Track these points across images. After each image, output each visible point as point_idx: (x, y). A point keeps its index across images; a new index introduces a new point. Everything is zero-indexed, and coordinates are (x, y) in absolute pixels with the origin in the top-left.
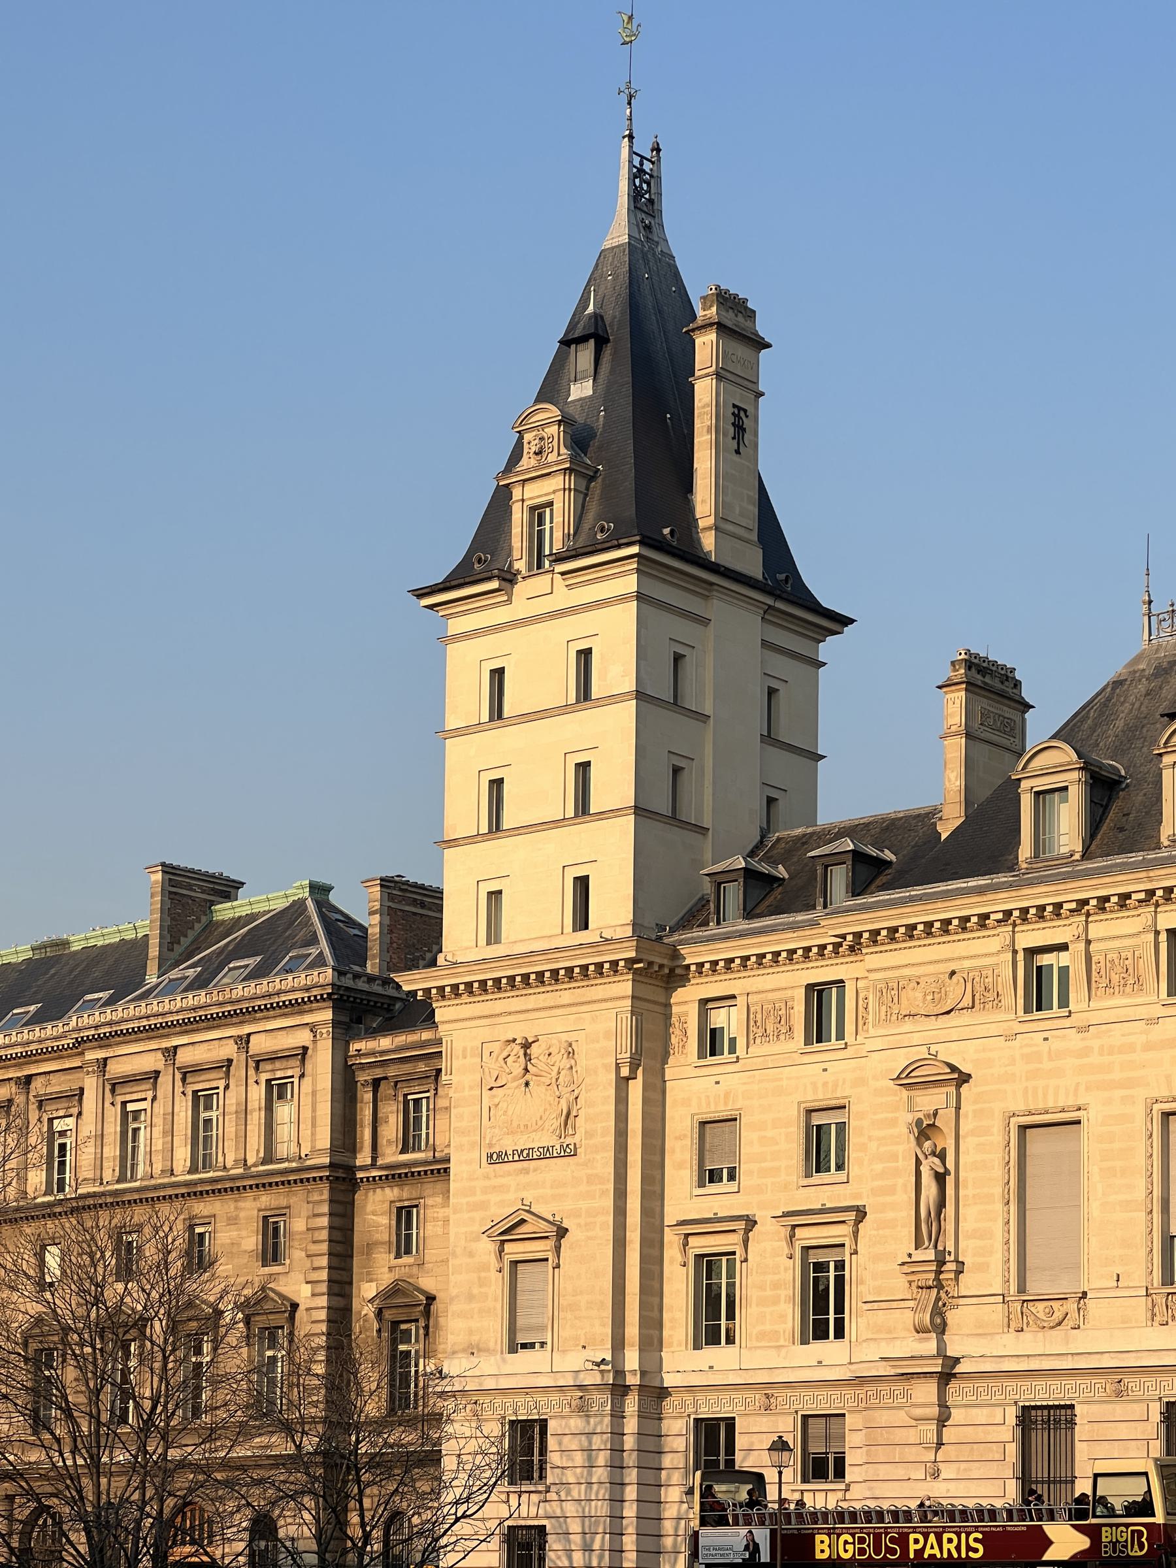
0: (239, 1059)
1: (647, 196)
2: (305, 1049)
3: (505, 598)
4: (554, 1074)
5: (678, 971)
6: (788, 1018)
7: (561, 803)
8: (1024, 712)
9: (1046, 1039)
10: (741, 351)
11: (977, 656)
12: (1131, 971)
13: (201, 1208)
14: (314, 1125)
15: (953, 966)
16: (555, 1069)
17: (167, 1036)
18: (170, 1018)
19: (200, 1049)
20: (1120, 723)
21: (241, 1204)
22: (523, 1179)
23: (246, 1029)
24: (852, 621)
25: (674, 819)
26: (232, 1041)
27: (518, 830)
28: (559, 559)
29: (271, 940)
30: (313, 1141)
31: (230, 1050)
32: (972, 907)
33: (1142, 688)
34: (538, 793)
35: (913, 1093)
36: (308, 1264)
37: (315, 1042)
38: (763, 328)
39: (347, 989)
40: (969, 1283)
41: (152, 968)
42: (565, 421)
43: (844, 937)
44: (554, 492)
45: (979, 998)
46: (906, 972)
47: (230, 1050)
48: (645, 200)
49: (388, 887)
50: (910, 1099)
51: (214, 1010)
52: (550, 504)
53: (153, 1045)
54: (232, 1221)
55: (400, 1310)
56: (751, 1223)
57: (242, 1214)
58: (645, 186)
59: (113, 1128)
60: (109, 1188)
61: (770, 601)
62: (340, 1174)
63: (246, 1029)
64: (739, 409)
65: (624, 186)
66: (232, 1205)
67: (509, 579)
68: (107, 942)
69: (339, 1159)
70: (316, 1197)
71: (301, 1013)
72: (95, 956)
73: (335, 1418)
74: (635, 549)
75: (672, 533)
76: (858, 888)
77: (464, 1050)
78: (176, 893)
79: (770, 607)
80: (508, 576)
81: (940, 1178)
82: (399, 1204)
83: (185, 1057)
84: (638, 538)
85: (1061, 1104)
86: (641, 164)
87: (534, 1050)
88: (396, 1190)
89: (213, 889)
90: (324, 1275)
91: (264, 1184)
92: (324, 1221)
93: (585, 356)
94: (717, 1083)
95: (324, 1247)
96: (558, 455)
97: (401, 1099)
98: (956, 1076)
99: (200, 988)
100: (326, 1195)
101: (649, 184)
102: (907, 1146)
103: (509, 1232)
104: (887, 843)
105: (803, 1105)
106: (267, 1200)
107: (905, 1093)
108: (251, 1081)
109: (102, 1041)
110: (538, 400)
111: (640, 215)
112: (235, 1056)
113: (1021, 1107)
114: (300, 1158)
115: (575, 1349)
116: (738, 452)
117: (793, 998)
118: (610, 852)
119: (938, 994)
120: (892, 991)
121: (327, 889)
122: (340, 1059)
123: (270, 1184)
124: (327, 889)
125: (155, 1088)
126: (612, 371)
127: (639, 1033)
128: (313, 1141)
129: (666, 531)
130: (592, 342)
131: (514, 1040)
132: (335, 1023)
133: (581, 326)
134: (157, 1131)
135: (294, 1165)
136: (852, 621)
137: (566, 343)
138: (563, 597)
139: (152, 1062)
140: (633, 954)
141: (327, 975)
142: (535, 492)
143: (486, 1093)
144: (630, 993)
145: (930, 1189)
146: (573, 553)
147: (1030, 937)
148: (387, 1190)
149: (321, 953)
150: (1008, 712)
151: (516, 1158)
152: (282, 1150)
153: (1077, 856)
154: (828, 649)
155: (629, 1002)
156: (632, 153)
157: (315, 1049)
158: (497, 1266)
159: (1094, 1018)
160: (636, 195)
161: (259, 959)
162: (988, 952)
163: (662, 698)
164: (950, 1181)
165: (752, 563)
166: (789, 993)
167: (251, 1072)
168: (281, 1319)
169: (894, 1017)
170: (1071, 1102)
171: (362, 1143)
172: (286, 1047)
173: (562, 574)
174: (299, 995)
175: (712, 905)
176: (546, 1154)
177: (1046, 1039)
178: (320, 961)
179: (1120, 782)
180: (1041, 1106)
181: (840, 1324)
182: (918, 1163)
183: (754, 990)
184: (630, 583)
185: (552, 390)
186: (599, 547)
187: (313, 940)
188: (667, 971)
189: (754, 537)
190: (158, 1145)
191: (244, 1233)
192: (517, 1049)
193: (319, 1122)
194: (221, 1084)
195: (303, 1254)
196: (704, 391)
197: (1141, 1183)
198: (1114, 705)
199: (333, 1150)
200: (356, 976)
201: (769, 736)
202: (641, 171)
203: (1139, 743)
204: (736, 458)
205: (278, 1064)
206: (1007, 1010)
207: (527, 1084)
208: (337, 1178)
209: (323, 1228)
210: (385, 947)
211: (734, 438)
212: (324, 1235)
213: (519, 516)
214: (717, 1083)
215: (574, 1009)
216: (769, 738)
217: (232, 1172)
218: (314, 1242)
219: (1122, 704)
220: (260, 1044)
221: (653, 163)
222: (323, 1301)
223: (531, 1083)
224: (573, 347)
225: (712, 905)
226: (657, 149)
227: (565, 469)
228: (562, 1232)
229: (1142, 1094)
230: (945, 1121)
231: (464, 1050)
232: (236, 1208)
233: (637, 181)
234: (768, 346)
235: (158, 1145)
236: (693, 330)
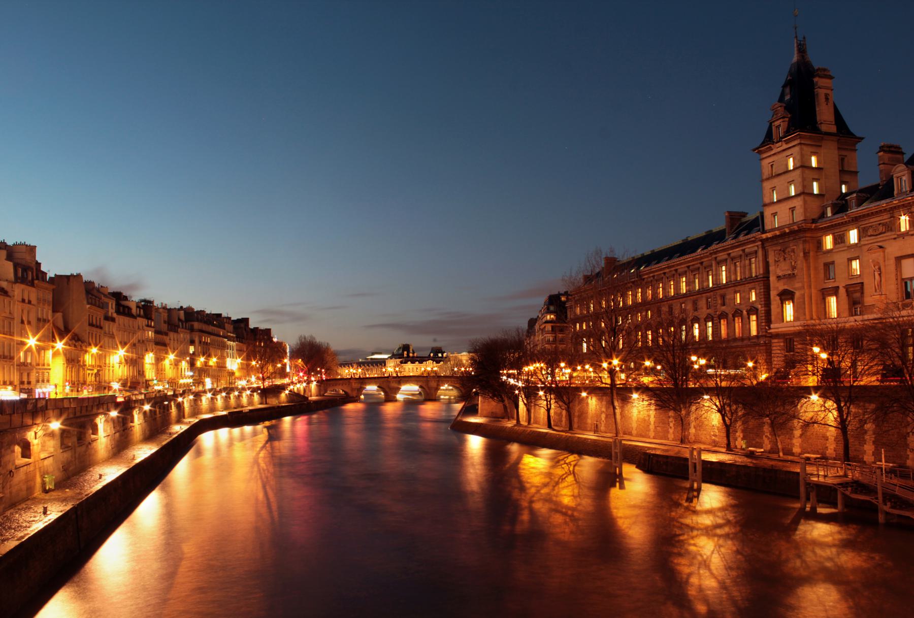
19: (736, 252)
24: (862, 138)
83: (732, 255)
106: (750, 286)
109: (715, 253)
165: (833, 129)
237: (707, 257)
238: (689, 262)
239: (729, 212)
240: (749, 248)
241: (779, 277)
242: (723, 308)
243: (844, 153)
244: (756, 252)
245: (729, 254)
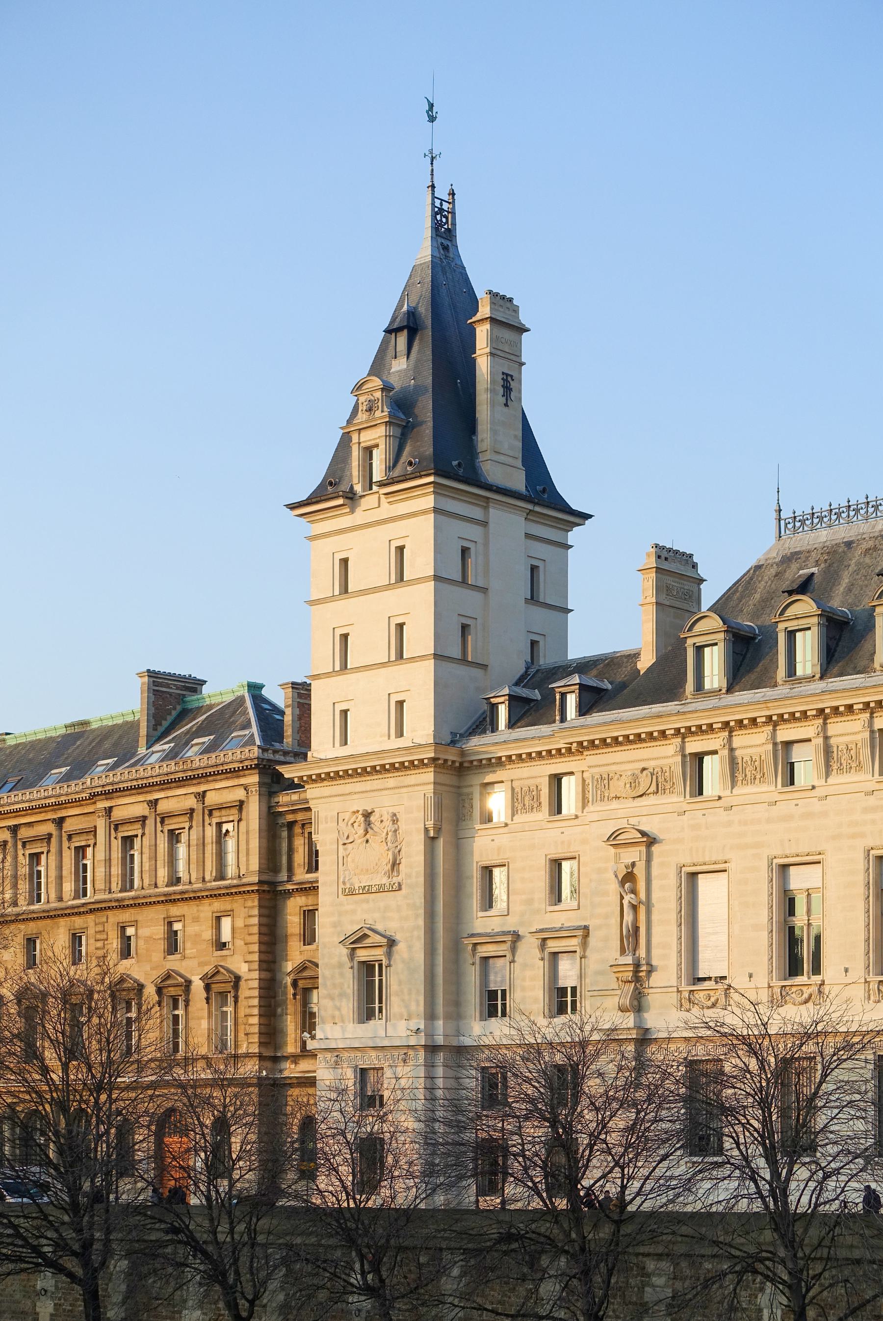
0: (198, 807)
1: (446, 227)
2: (242, 803)
3: (348, 510)
4: (384, 834)
5: (466, 765)
6: (539, 796)
7: (382, 652)
8: (699, 584)
9: (704, 815)
10: (507, 334)
11: (663, 548)
12: (758, 769)
13: (175, 910)
14: (248, 854)
16: (385, 831)
17: (150, 792)
18: (151, 780)
19: (175, 801)
20: (757, 596)
21: (201, 908)
22: (365, 906)
23: (202, 788)
24: (590, 516)
25: (463, 660)
26: (193, 796)
27: (357, 669)
28: (382, 484)
29: (222, 722)
30: (248, 865)
31: (191, 802)
32: (655, 727)
33: (773, 571)
34: (371, 645)
35: (619, 850)
36: (245, 947)
37: (247, 797)
38: (524, 318)
39: (269, 760)
40: (656, 980)
41: (143, 741)
42: (386, 388)
43: (571, 744)
44: (379, 437)
45: (659, 785)
46: (614, 768)
47: (191, 802)
48: (444, 232)
49: (297, 689)
50: (616, 854)
51: (180, 775)
52: (377, 446)
53: (141, 798)
54: (196, 920)
55: (308, 981)
56: (516, 937)
57: (202, 915)
58: (444, 220)
59: (117, 854)
60: (114, 895)
61: (530, 507)
62: (266, 888)
63: (202, 788)
64: (507, 375)
65: (428, 223)
66: (195, 909)
67: (351, 497)
68: (115, 723)
69: (265, 877)
70: (249, 903)
71: (238, 777)
72: (107, 733)
73: (267, 1053)
74: (431, 479)
75: (459, 465)
76: (584, 710)
77: (326, 818)
78: (157, 691)
79: (530, 510)
80: (350, 495)
81: (634, 908)
82: (305, 908)
83: (162, 807)
84: (432, 471)
85: (714, 859)
86: (441, 204)
87: (372, 818)
88: (304, 898)
89: (184, 686)
90: (256, 957)
91: (214, 896)
92: (255, 920)
93: (402, 339)
94: (493, 840)
95: (256, 938)
96: (382, 414)
97: (306, 835)
98: (645, 839)
99: (171, 759)
100: (256, 903)
101: (447, 218)
102: (614, 887)
103: (358, 940)
104: (607, 675)
105: (549, 857)
106: (218, 905)
107: (612, 850)
108: (206, 823)
109: (108, 795)
110: (369, 375)
111: (440, 240)
112: (195, 807)
113: (688, 861)
114: (239, 877)
115: (403, 1019)
116: (506, 405)
117: (541, 784)
118: (418, 685)
119: (634, 782)
120: (605, 780)
121: (260, 687)
122: (265, 809)
123: (220, 895)
124: (260, 687)
126: (419, 352)
127: (439, 806)
128: (248, 865)
129: (455, 463)
130: (405, 332)
131: (358, 811)
132: (261, 784)
133: (398, 320)
134: (146, 857)
135: (235, 882)
136: (590, 516)
137: (388, 331)
138: (387, 510)
139: (141, 810)
140: (432, 755)
141: (256, 752)
142: (368, 437)
143: (341, 847)
144: (432, 780)
145: (628, 917)
146: (391, 481)
148: (298, 898)
149: (253, 735)
150: (687, 586)
151: (361, 891)
152: (231, 871)
153: (724, 691)
154: (574, 536)
155: (432, 786)
156: (434, 197)
157: (248, 802)
158: (349, 965)
159: (734, 801)
160: (437, 227)
161: (212, 737)
162: (666, 756)
163: (457, 574)
164: (642, 910)
165: (518, 481)
166: (538, 781)
167: (207, 817)
168: (229, 987)
169: (606, 798)
170: (721, 858)
171: (281, 866)
172: (229, 800)
173: (385, 494)
174: (236, 765)
175: (488, 719)
176: (381, 890)
177: (704, 815)
178: (251, 741)
179: (754, 638)
180: (701, 860)
181: (574, 1003)
182: (622, 898)
183: (516, 778)
184: (428, 501)
185: (378, 367)
186: (408, 477)
187: (247, 725)
188: (457, 764)
189: (519, 463)
190: (146, 867)
191: (204, 928)
192: (361, 819)
193: (251, 852)
194: (187, 825)
195: (242, 943)
196: (483, 364)
197: (765, 912)
198: (755, 583)
199: (260, 872)
200: (275, 752)
201: (532, 598)
202: (441, 210)
203: (768, 610)
204: (506, 409)
205: (224, 812)
206: (679, 794)
207: (367, 841)
208: (264, 891)
209: (255, 925)
210: (296, 729)
211: (503, 396)
212: (255, 930)
213: (355, 452)
214: (493, 840)
215: (397, 791)
216: (533, 599)
217: (195, 886)
218: (250, 934)
219: (759, 582)
220: (212, 799)
221: (449, 203)
222: (256, 975)
223: (370, 841)
224: (393, 334)
225: (488, 719)
226: (452, 194)
227: (386, 422)
228: (392, 943)
229: (767, 852)
230: (640, 872)
231: (326, 818)
232: (198, 911)
233: (438, 217)
234: (527, 330)
235: (146, 867)
236: (474, 322)
237: (78, 802)
238: (17, 813)
239: (151, 674)
240: (221, 793)
242: (125, 966)
243: (541, 550)
244: (241, 805)
245: (154, 804)
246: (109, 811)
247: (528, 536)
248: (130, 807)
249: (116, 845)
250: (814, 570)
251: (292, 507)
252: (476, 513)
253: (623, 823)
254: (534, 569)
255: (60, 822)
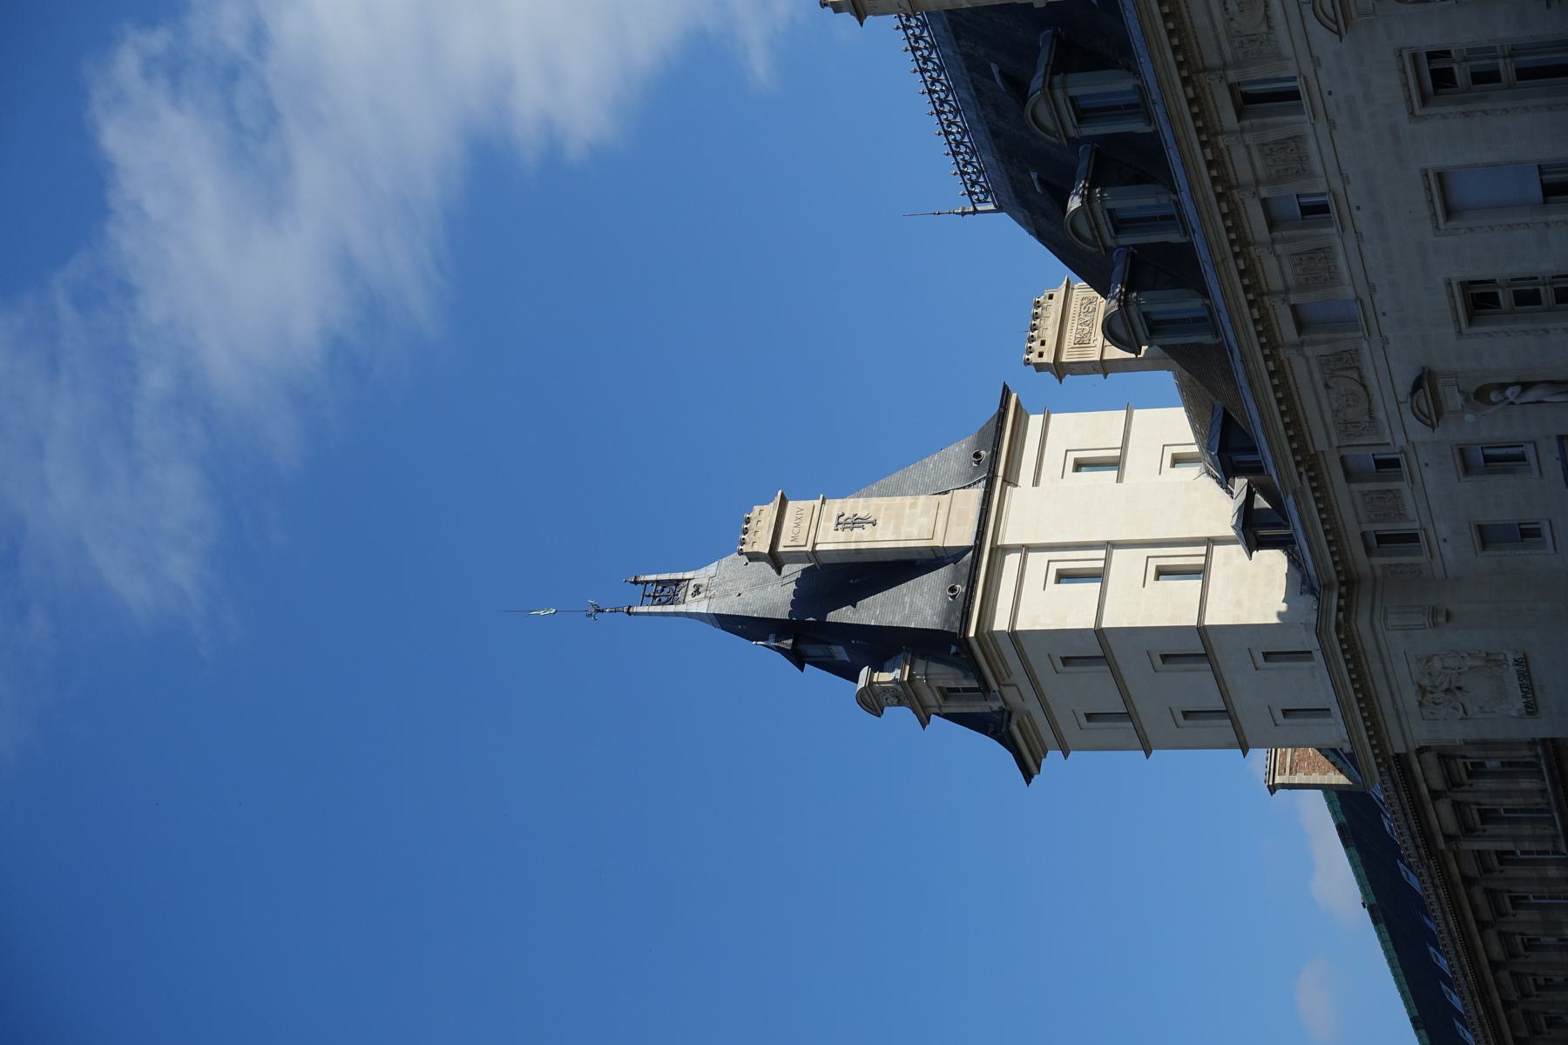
15: (1320, 386)
24: (1005, 386)
53: (1430, 807)
61: (999, 481)
79: (1004, 480)
81: (1526, 386)
87: (1425, 682)
125: (1468, 804)
136: (1005, 386)
139: (1445, 807)
147: (1287, 329)
188: (1343, 590)
207: (1459, 688)
241: (1531, 709)
245: (1435, 795)
246: (1448, 838)
247: (1036, 483)
248: (1442, 817)
249: (1492, 829)
250: (1034, 175)
251: (1028, 777)
252: (1012, 561)
253: (1406, 408)
254: (1079, 466)
255: (1468, 881)
